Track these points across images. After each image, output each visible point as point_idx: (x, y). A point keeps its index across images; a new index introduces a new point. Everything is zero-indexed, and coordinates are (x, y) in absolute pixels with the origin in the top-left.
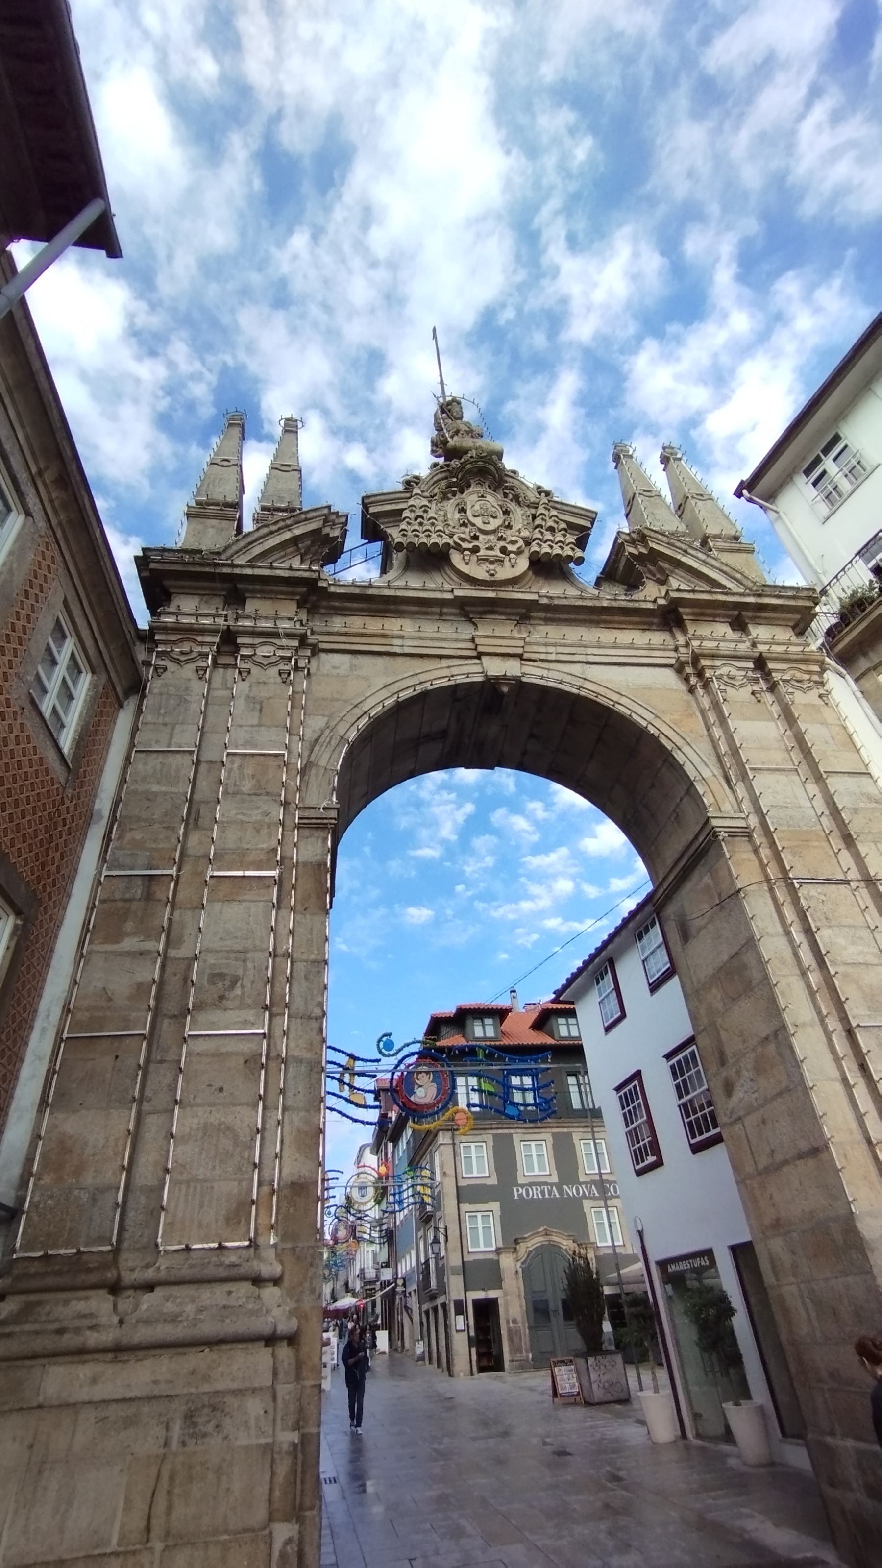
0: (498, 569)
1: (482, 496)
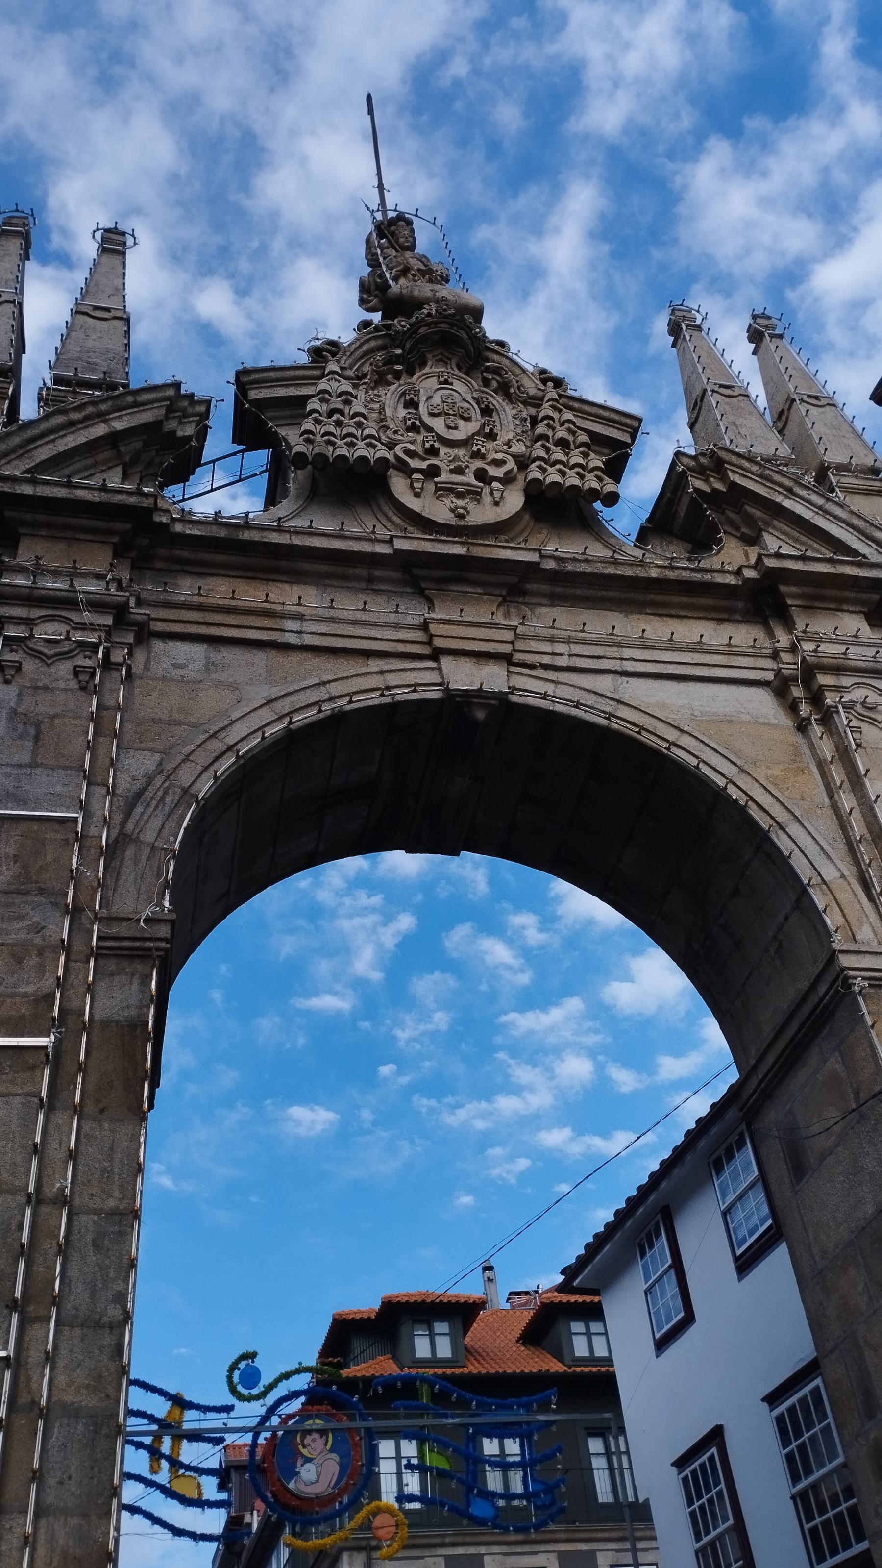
1: (446, 382)
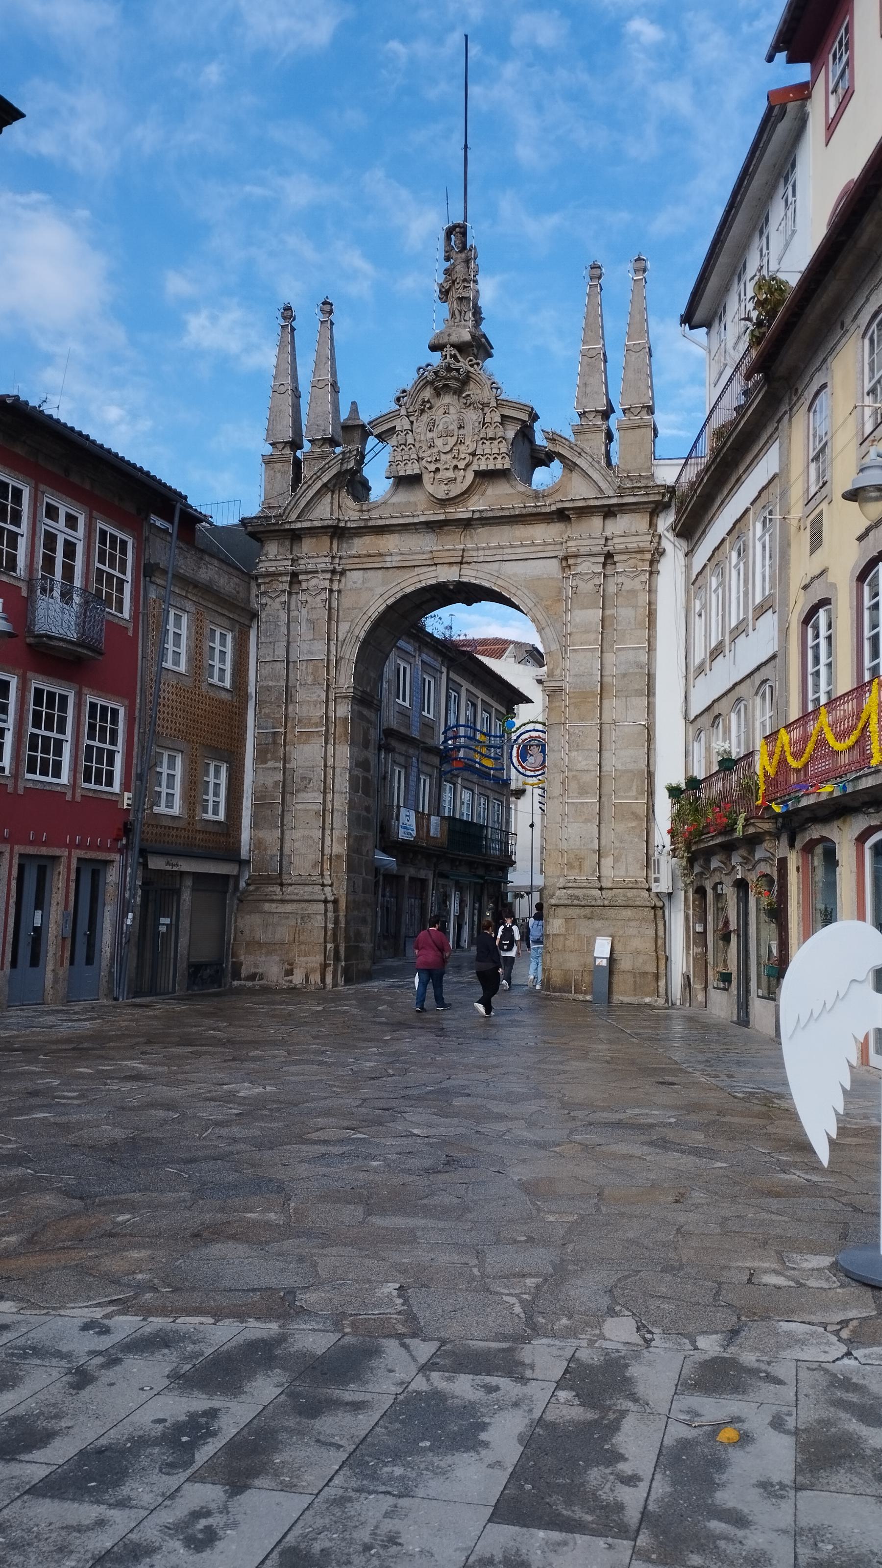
0: (451, 486)
1: (445, 413)
